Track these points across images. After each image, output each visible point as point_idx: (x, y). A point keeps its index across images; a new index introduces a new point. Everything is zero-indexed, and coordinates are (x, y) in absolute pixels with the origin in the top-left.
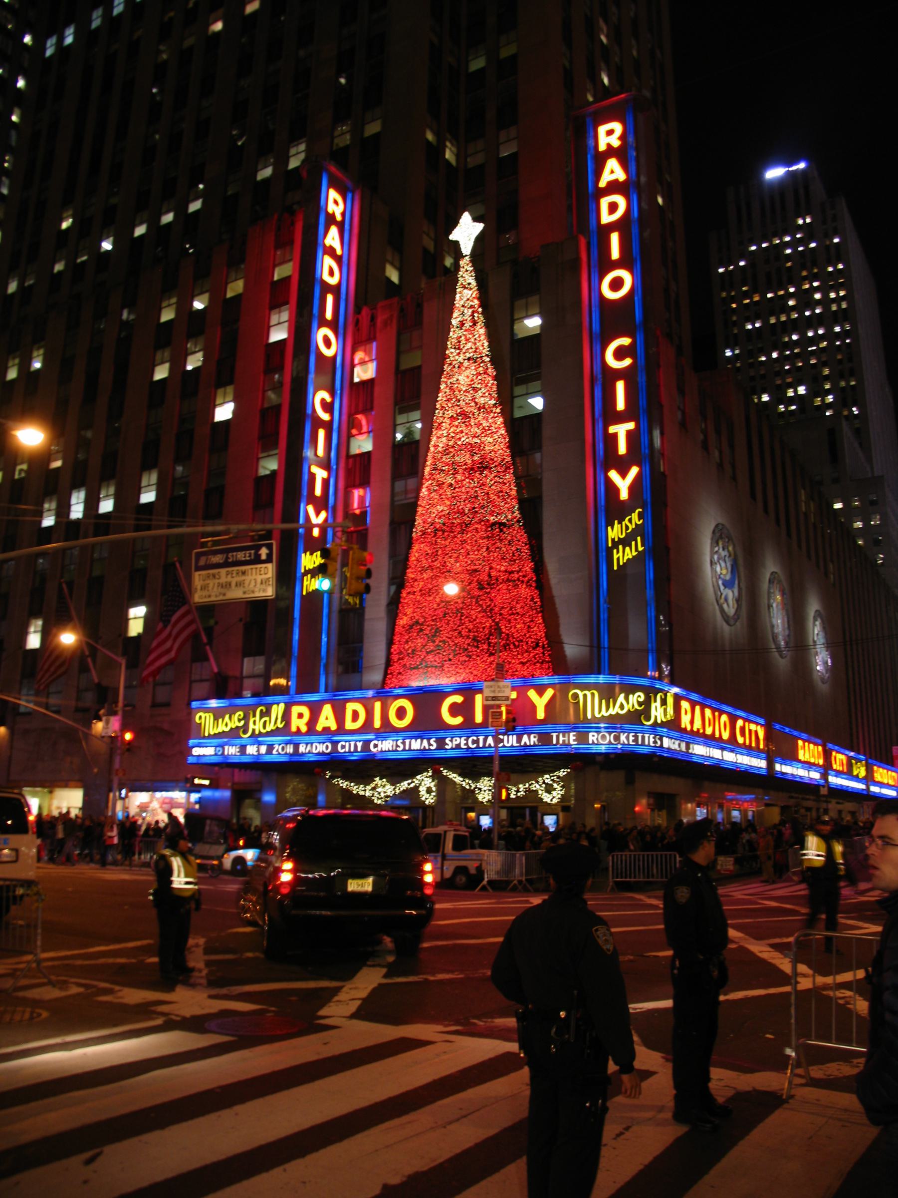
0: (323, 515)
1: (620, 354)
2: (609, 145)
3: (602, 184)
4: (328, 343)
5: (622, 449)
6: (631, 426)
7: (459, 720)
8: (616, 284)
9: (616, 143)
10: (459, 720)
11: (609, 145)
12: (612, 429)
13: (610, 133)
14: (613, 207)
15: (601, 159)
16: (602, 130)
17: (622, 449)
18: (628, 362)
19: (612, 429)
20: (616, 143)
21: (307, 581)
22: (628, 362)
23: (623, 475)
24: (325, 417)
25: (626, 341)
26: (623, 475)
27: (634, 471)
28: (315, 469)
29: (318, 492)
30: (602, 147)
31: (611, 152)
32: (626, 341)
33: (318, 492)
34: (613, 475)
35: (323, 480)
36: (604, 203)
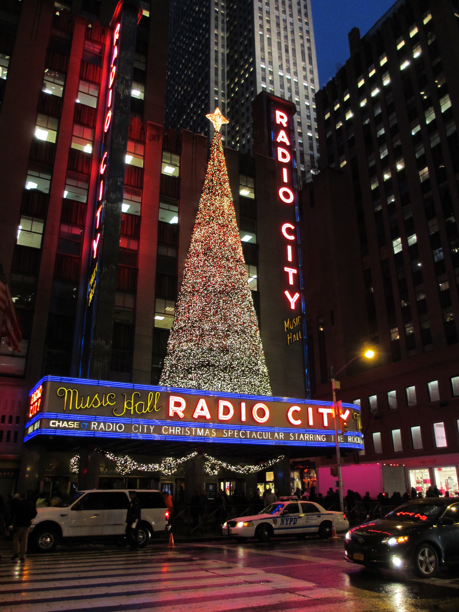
0: (297, 296)
4: (286, 195)
21: (290, 336)
24: (292, 238)
28: (286, 269)
29: (291, 282)
33: (291, 282)
35: (294, 274)
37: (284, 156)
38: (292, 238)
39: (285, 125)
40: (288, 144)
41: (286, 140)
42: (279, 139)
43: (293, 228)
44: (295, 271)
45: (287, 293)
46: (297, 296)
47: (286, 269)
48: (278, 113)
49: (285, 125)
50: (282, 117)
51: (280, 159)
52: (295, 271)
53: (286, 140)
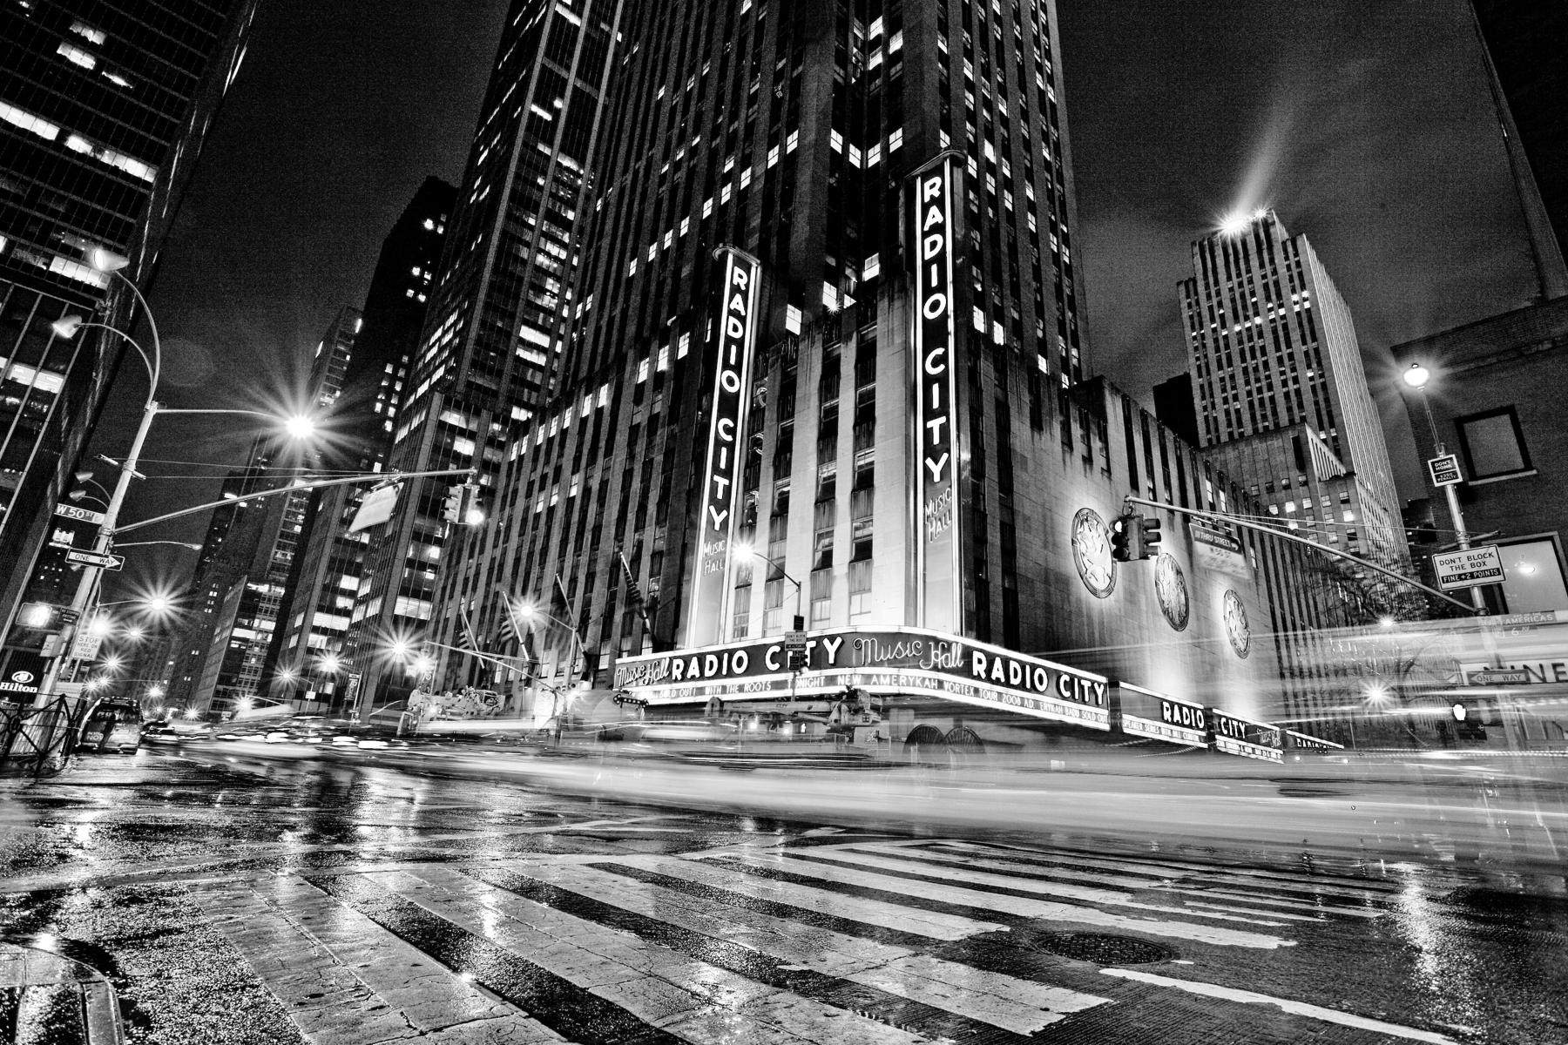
1: (935, 364)
2: (932, 196)
3: (926, 229)
4: (731, 382)
5: (936, 441)
6: (943, 420)
7: (777, 666)
8: (935, 306)
9: (937, 193)
10: (777, 666)
11: (932, 196)
12: (929, 425)
13: (932, 186)
14: (934, 245)
15: (926, 208)
16: (927, 184)
17: (936, 441)
18: (942, 367)
19: (929, 425)
20: (937, 193)
22: (942, 367)
23: (936, 462)
24: (729, 438)
25: (940, 351)
26: (936, 462)
27: (945, 456)
29: (720, 496)
30: (927, 199)
31: (934, 201)
32: (940, 351)
33: (720, 496)
34: (929, 462)
36: (928, 241)
37: (735, 329)
38: (729, 438)
39: (743, 288)
40: (743, 313)
41: (741, 308)
42: (732, 307)
43: (732, 425)
44: (727, 482)
45: (712, 508)
46: (724, 513)
47: (716, 478)
48: (738, 270)
49: (743, 288)
50: (741, 276)
51: (731, 333)
52: (727, 482)
53: (741, 308)
